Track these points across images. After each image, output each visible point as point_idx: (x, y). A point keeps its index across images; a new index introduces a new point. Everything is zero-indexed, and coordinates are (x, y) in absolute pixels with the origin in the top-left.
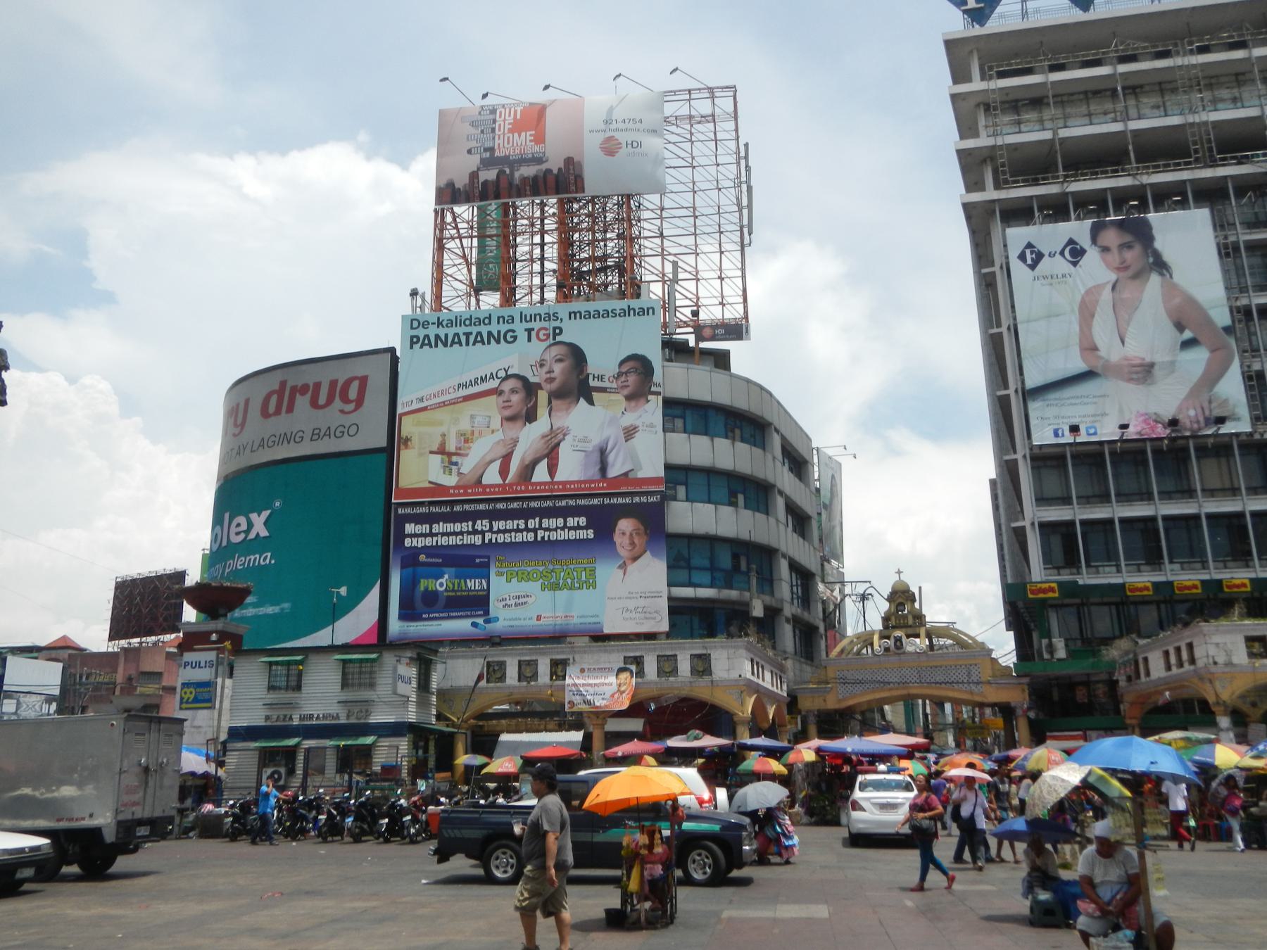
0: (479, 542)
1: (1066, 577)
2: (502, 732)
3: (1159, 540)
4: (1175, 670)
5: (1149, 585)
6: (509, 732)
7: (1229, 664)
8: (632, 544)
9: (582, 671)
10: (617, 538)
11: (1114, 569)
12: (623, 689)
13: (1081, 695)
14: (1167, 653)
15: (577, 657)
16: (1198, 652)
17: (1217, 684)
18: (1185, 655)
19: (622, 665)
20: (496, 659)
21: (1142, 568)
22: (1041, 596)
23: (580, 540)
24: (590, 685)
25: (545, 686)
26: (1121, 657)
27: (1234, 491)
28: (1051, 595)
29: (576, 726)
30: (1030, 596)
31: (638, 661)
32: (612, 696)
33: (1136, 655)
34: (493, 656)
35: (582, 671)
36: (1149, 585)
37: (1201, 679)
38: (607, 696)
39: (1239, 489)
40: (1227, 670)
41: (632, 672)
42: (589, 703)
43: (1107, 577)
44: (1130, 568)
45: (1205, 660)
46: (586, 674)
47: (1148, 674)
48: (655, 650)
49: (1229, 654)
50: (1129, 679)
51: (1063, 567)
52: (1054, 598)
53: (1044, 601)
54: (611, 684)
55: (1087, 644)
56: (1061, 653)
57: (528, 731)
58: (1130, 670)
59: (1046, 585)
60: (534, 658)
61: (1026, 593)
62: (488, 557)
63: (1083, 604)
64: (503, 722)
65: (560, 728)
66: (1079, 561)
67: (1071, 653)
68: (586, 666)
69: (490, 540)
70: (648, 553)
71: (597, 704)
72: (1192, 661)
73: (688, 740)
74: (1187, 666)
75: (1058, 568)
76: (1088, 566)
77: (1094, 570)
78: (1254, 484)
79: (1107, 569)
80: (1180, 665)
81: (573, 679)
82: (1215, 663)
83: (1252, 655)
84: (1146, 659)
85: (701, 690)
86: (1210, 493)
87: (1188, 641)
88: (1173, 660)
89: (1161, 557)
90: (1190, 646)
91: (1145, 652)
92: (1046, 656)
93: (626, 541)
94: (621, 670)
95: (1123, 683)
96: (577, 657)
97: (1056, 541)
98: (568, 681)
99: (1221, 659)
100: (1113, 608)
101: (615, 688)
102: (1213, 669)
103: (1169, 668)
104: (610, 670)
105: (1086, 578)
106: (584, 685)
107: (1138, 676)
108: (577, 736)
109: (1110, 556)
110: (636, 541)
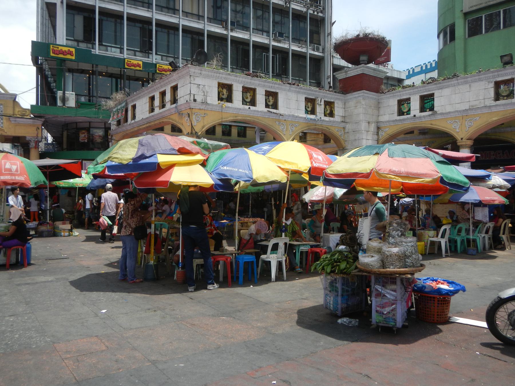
1: (83, 46)
3: (151, 38)
4: (157, 111)
5: (141, 63)
7: (204, 103)
11: (118, 50)
13: (83, 137)
14: (152, 99)
16: (180, 93)
17: (194, 118)
18: (168, 97)
21: (137, 53)
22: (61, 56)
26: (116, 105)
27: (199, 17)
28: (69, 57)
30: (52, 54)
33: (127, 104)
36: (141, 63)
37: (180, 114)
39: (203, 17)
40: (203, 107)
43: (114, 52)
44: (129, 52)
45: (187, 98)
47: (134, 117)
49: (205, 95)
50: (119, 123)
51: (83, 42)
52: (71, 60)
53: (64, 60)
55: (89, 98)
56: (72, 103)
58: (121, 116)
59: (66, 49)
61: (49, 53)
63: (94, 73)
66: (95, 40)
67: (79, 105)
72: (174, 101)
74: (168, 106)
75: (78, 41)
76: (100, 44)
77: (104, 48)
78: (210, 17)
79: (113, 49)
80: (163, 105)
82: (195, 100)
83: (220, 99)
84: (134, 107)
86: (186, 14)
87: (173, 84)
88: (157, 102)
89: (151, 49)
90: (175, 89)
91: (133, 101)
92: (59, 103)
95: (113, 127)
97: (79, 20)
99: (199, 99)
100: (114, 80)
102: (193, 105)
103: (152, 110)
105: (97, 51)
107: (126, 120)
109: (118, 41)
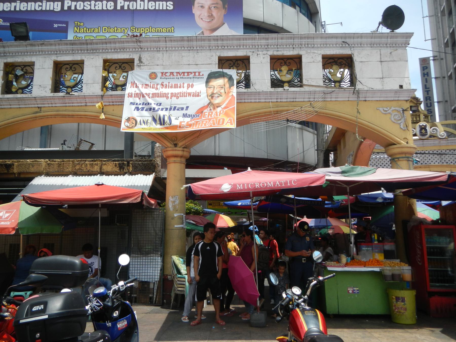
0: (59, 9)
2: (39, 174)
6: (48, 174)
8: (211, 16)
9: (153, 76)
10: (196, 10)
12: (217, 101)
15: (145, 56)
19: (215, 69)
20: (19, 60)
23: (159, 10)
24: (165, 95)
25: (93, 97)
29: (146, 167)
31: (242, 63)
32: (201, 111)
34: (14, 54)
35: (153, 76)
38: (192, 111)
41: (230, 78)
42: (162, 122)
46: (158, 81)
48: (267, 47)
54: (197, 95)
57: (75, 174)
60: (78, 58)
62: (67, 23)
64: (43, 161)
65: (122, 170)
68: (158, 70)
69: (69, 7)
70: (226, 25)
71: (175, 122)
73: (343, 172)
81: (137, 84)
85: (341, 106)
93: (205, 13)
94: (212, 76)
96: (145, 56)
98: (129, 89)
101: (204, 100)
104: (197, 75)
106: (154, 95)
108: (145, 181)
110: (214, 14)
